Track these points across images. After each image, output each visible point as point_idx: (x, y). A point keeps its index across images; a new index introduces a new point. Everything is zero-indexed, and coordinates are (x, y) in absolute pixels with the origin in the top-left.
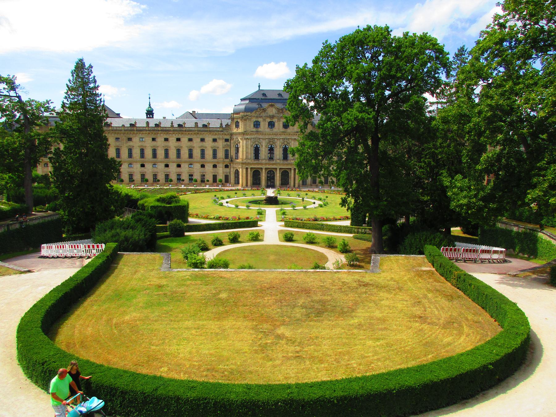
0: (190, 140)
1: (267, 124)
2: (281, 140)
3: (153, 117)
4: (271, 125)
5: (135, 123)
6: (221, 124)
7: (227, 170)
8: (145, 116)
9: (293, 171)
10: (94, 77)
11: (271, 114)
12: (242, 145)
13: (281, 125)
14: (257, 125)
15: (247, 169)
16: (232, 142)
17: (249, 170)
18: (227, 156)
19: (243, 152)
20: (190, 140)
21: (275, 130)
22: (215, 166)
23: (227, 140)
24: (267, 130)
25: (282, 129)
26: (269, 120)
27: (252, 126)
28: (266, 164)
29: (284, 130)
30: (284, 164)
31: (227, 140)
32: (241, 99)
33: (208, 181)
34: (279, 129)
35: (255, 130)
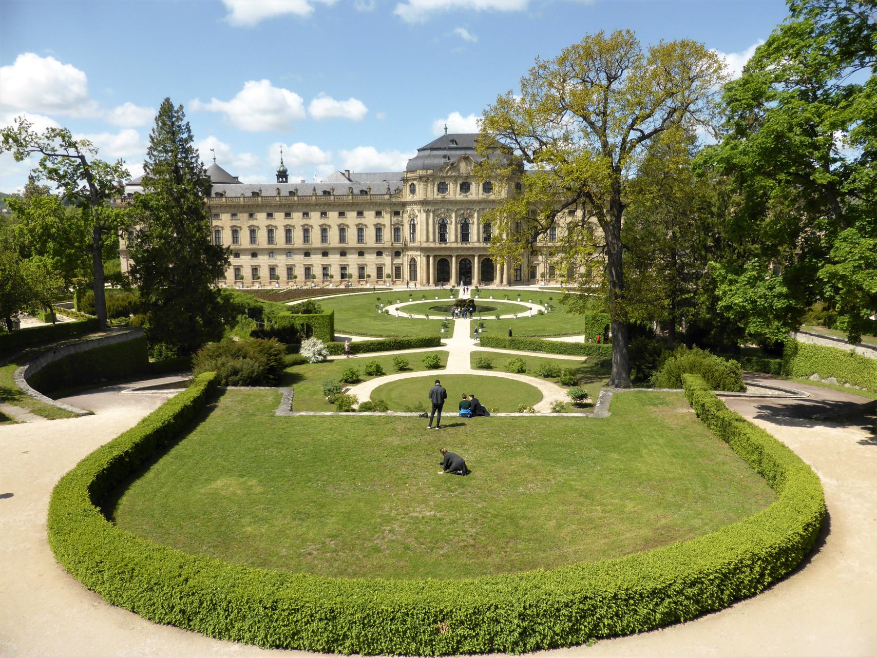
3: (286, 181)
5: (260, 191)
6: (389, 189)
8: (274, 181)
10: (188, 124)
12: (421, 218)
16: (405, 216)
17: (431, 259)
18: (397, 239)
19: (421, 230)
28: (457, 249)
29: (485, 196)
31: (397, 213)
32: (419, 150)
33: (369, 276)
34: (478, 194)
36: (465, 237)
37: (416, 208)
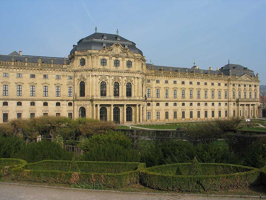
0: (33, 76)
1: (113, 62)
2: (125, 78)
4: (117, 63)
7: (71, 108)
9: (138, 107)
11: (117, 53)
13: (125, 64)
14: (104, 62)
15: (96, 105)
16: (76, 79)
17: (99, 106)
20: (33, 76)
21: (120, 68)
22: (58, 104)
23: (71, 78)
24: (113, 68)
25: (125, 68)
26: (114, 58)
27: (99, 63)
30: (130, 100)
31: (71, 78)
34: (123, 68)
35: (101, 67)
36: (116, 94)
37: (84, 74)
